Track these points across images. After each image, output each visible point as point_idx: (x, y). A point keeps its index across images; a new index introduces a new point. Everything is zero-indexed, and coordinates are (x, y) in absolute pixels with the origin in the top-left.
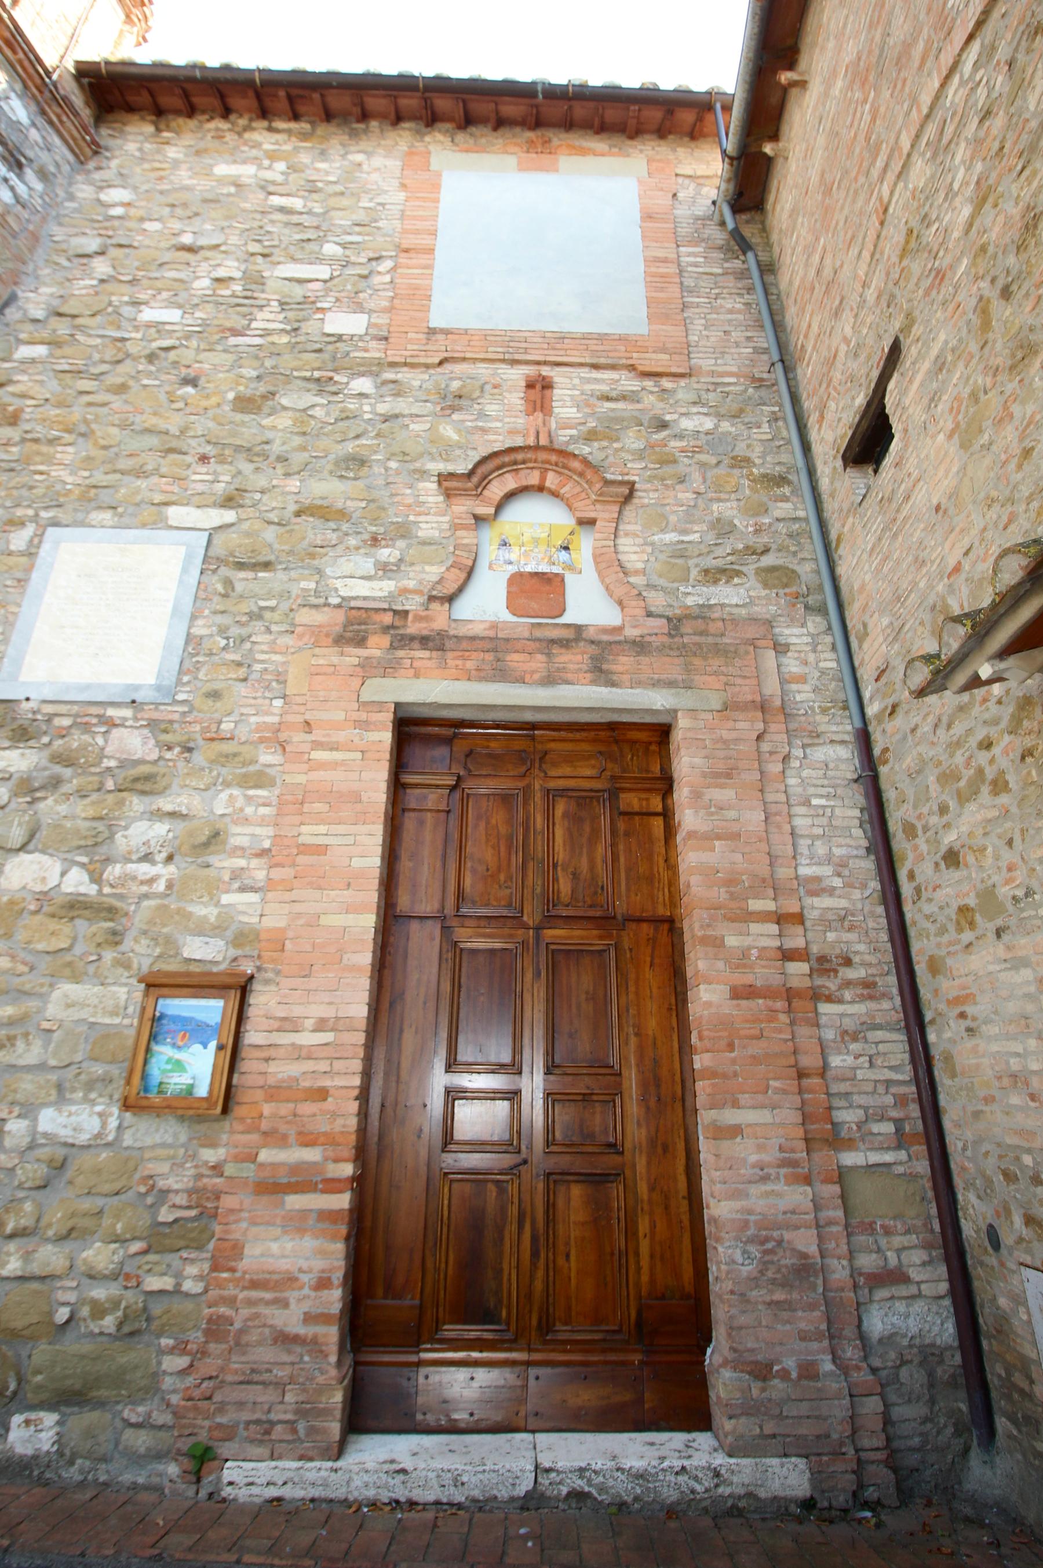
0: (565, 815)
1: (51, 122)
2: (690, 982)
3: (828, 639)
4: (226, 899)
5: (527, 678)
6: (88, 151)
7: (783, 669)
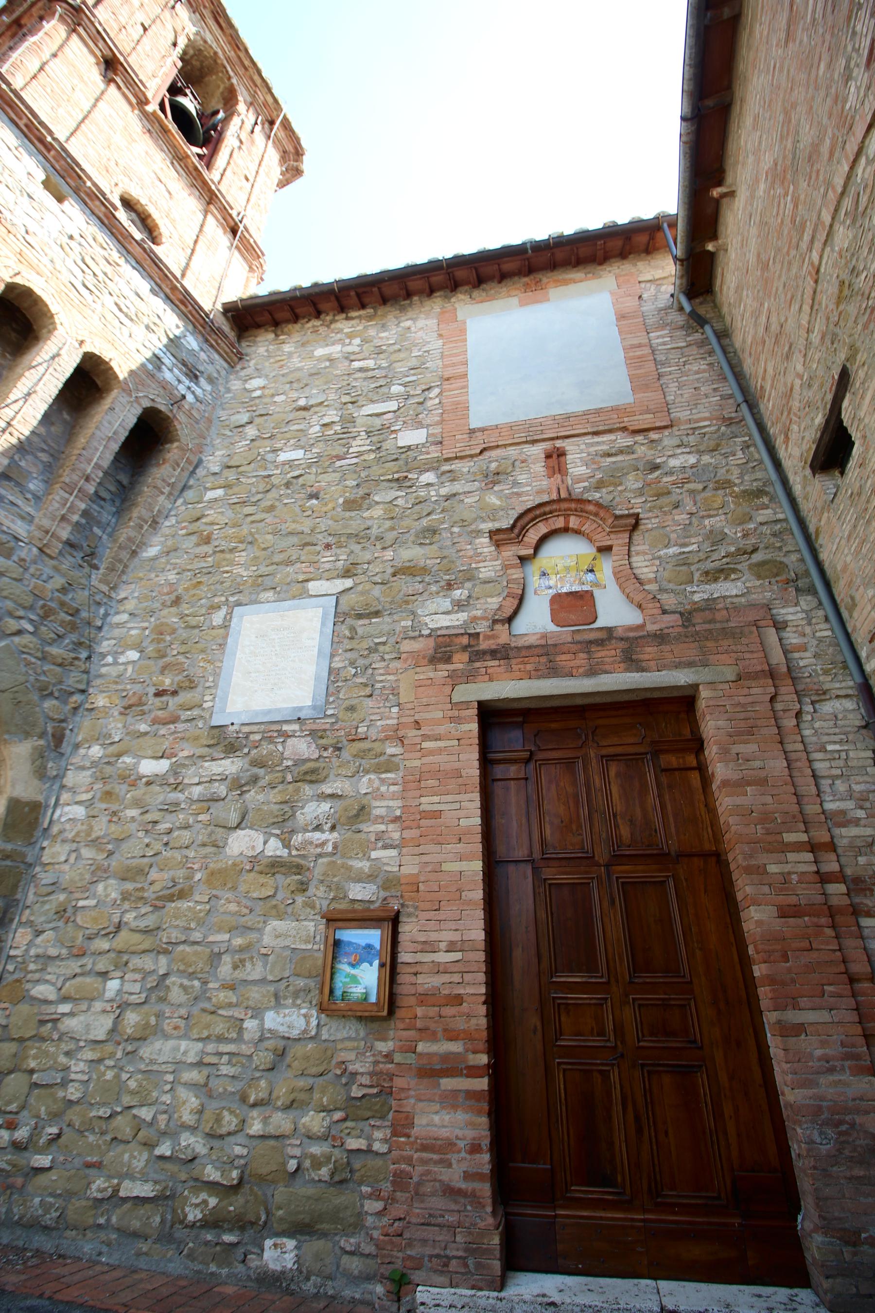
0: (618, 775)
1: (212, 346)
2: (741, 905)
3: (821, 613)
4: (374, 855)
5: (574, 672)
6: (235, 359)
7: (785, 642)
